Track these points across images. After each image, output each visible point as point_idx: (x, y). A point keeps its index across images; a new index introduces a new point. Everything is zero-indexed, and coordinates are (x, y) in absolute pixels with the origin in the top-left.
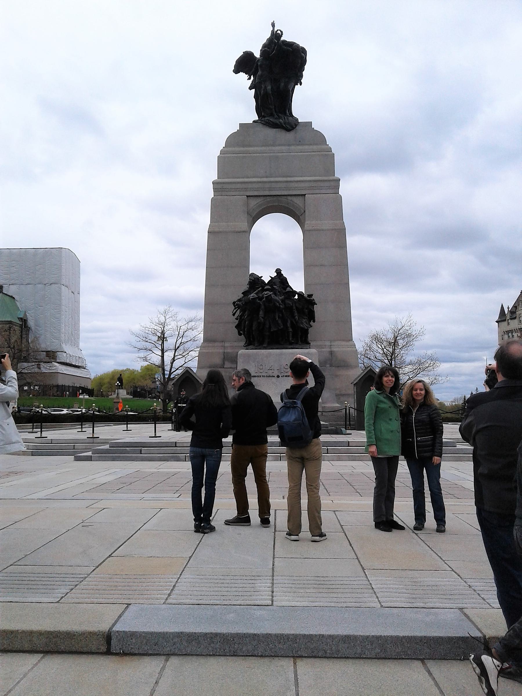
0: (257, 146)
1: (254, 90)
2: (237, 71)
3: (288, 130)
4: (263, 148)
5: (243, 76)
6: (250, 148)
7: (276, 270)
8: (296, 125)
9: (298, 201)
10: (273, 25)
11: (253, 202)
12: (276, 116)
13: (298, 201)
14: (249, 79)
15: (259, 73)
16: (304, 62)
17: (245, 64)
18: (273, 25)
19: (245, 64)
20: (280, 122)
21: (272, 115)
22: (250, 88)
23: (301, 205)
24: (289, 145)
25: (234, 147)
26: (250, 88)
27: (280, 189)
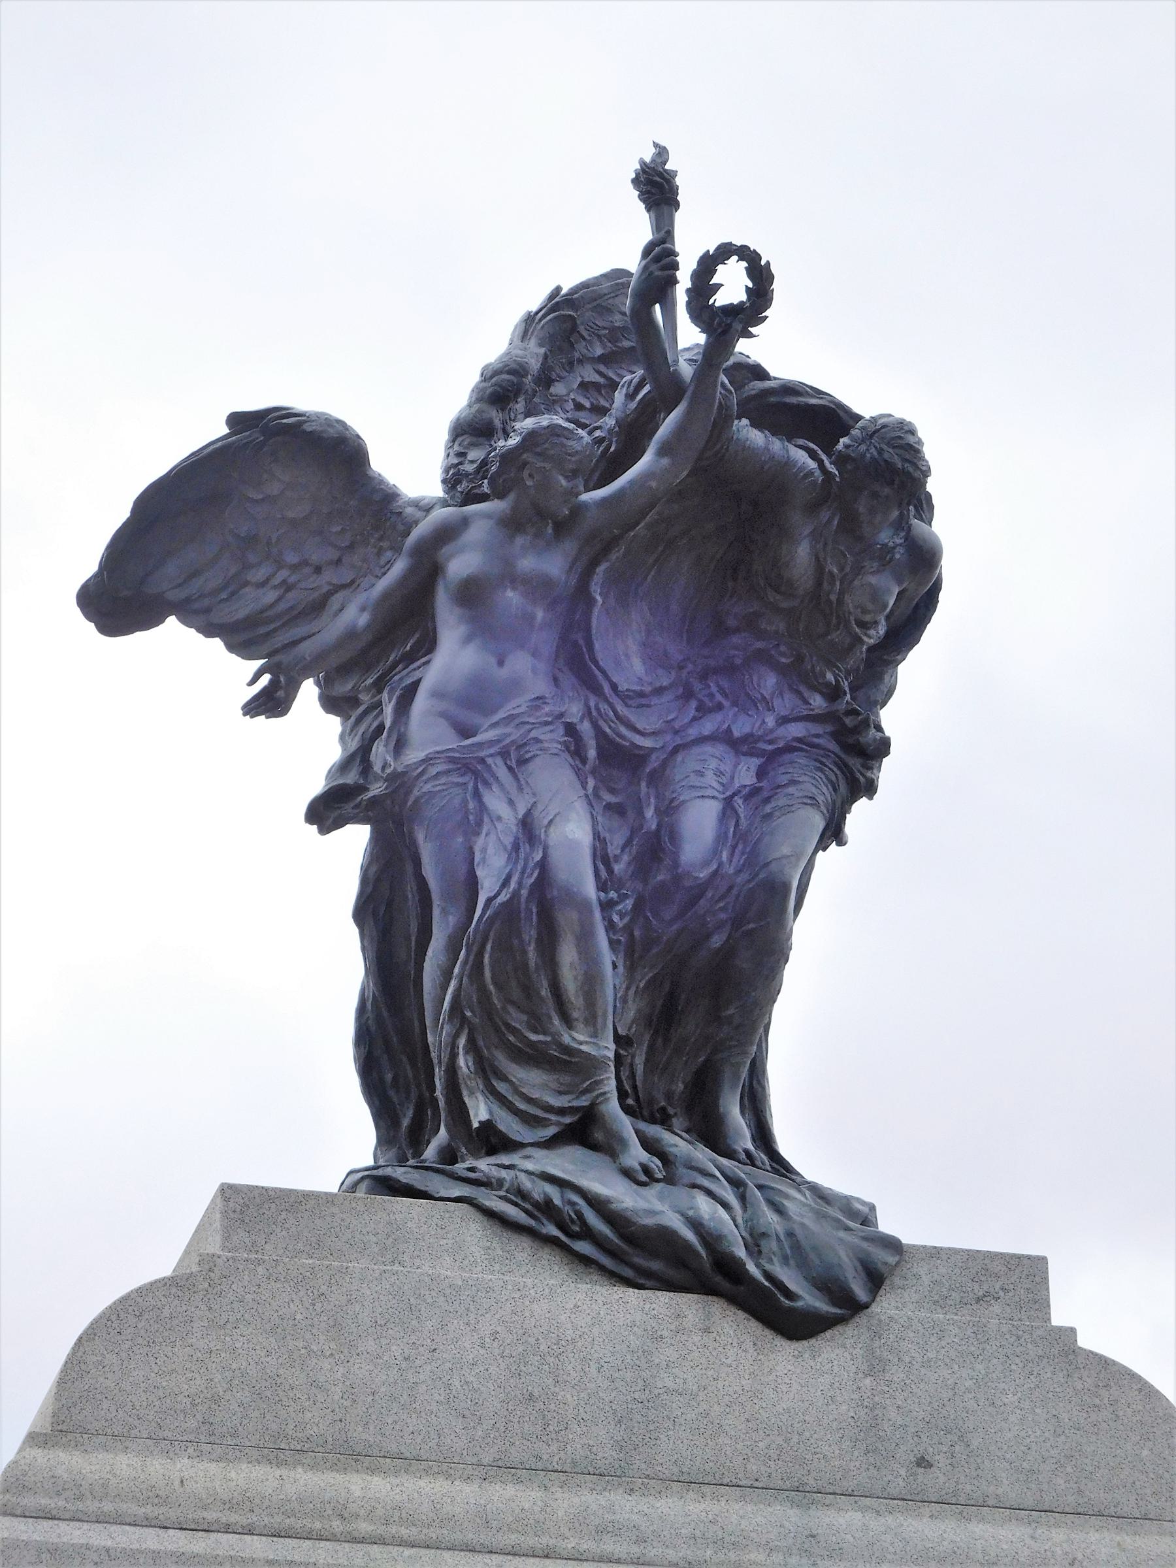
0: (443, 1464)
3: (790, 1323)
4: (505, 1496)
6: (358, 1486)
8: (876, 1279)
10: (657, 188)
12: (636, 1155)
14: (271, 703)
15: (454, 656)
17: (239, 537)
18: (657, 188)
19: (239, 537)
20: (696, 1225)
21: (584, 1131)
22: (327, 812)
24: (803, 1493)
25: (163, 1442)
26: (327, 812)
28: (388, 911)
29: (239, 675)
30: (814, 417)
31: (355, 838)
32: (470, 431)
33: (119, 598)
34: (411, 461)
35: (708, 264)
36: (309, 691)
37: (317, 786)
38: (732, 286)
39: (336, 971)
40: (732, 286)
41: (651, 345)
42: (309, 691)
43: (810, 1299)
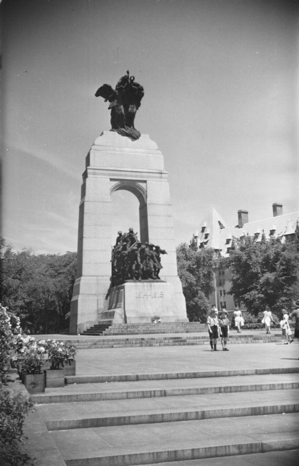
1: (111, 110)
2: (97, 95)
5: (101, 99)
7: (130, 229)
9: (143, 185)
10: (128, 72)
11: (115, 183)
13: (143, 185)
14: (106, 101)
16: (143, 95)
17: (104, 92)
18: (128, 72)
19: (104, 92)
22: (109, 108)
23: (145, 188)
26: (109, 108)
27: (132, 176)
28: (113, 114)
29: (104, 99)
30: (138, 85)
31: (111, 110)
32: (117, 86)
33: (97, 95)
34: (114, 88)
35: (131, 77)
36: (108, 101)
37: (108, 107)
38: (132, 78)
39: (110, 117)
40: (132, 78)
41: (128, 82)
42: (108, 101)
43: (136, 137)
